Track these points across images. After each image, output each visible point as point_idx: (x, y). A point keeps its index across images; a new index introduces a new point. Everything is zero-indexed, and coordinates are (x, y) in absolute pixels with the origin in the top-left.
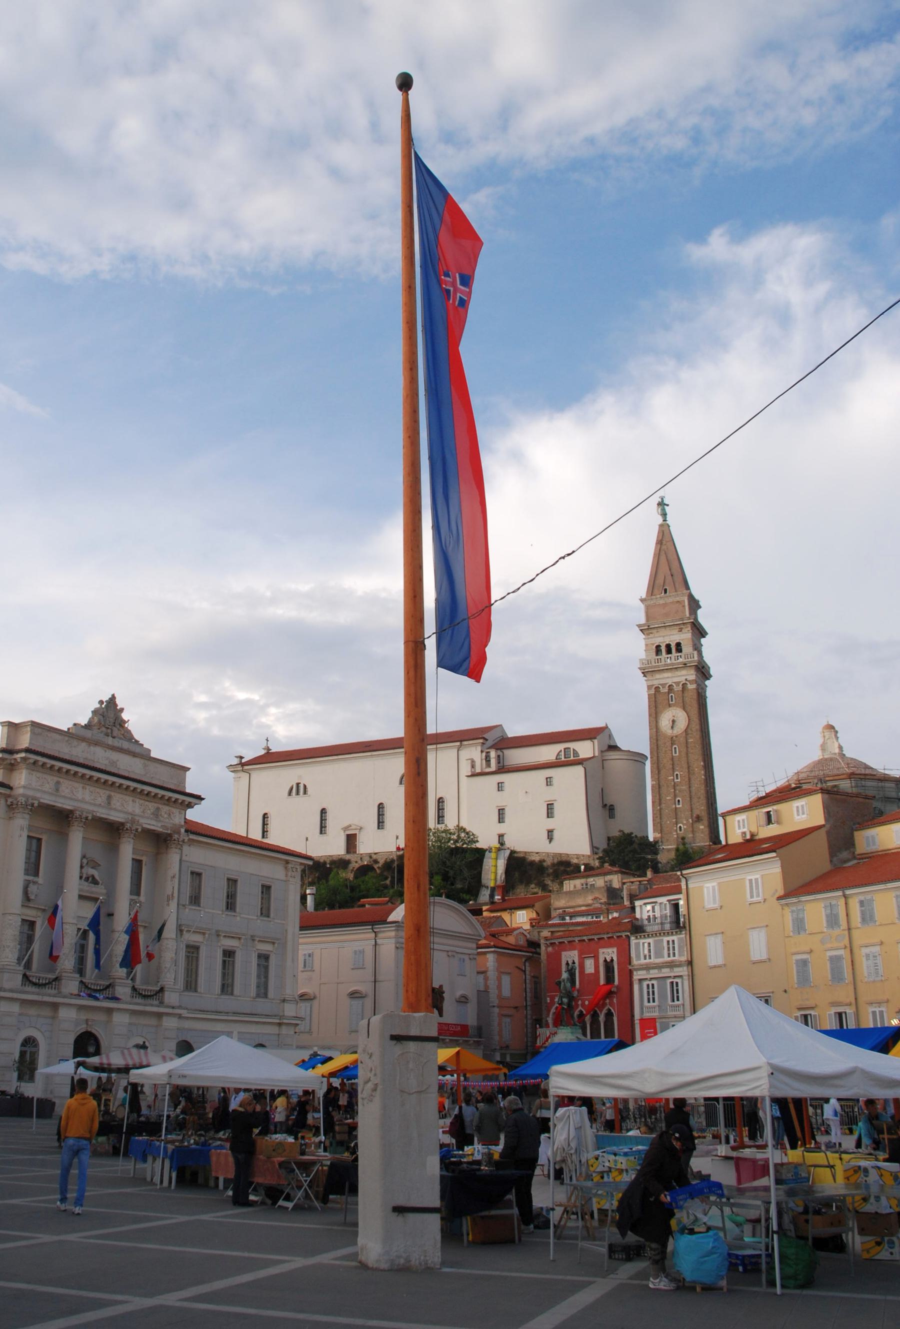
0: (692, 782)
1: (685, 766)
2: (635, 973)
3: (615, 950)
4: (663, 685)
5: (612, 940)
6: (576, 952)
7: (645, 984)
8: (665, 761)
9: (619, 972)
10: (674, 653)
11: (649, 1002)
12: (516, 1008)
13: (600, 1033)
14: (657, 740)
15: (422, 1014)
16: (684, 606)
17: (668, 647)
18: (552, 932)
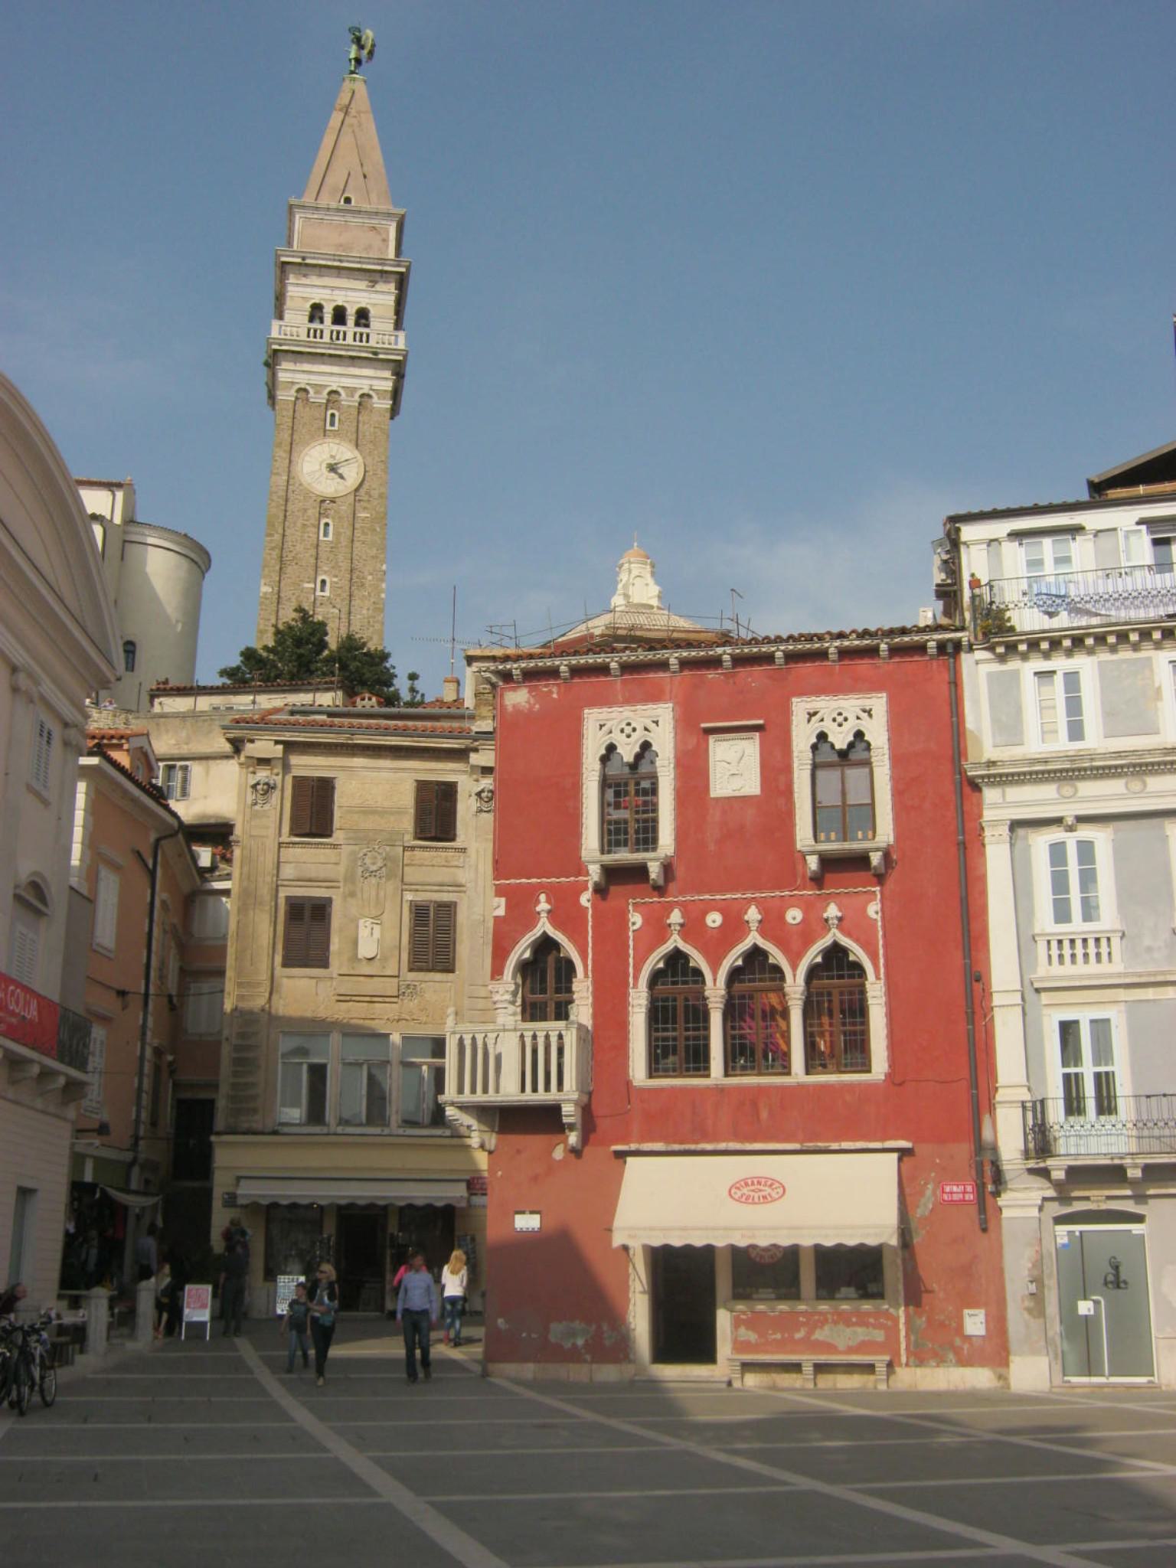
0: (356, 602)
1: (345, 565)
2: (990, 795)
3: (879, 703)
4: (319, 388)
5: (863, 665)
6: (665, 712)
7: (1041, 842)
8: (299, 548)
9: (898, 793)
10: (350, 327)
11: (1062, 913)
12: (122, 993)
13: (786, 1056)
14: (287, 500)
15: (326, 699)
16: (385, 241)
17: (339, 316)
18: (290, 747)
